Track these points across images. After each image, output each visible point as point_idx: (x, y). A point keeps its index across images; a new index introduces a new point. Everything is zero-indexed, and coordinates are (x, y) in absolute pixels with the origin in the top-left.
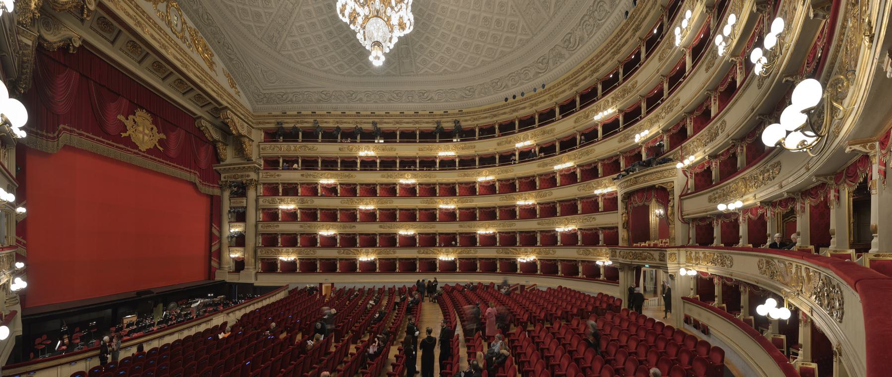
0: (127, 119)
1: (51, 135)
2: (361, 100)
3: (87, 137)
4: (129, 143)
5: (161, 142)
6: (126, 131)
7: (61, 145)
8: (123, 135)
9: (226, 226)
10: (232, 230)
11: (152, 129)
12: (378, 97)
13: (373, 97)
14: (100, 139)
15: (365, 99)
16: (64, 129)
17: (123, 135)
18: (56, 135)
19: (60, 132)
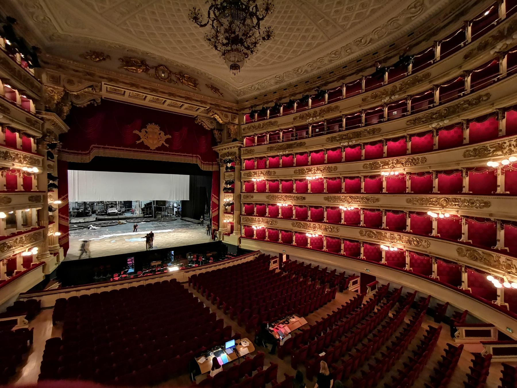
0: (140, 132)
1: (84, 152)
2: (306, 71)
3: (111, 149)
4: (143, 147)
5: (167, 141)
6: (139, 138)
7: (92, 158)
8: (138, 142)
9: (222, 194)
10: (225, 200)
11: (160, 134)
12: (319, 64)
13: (315, 65)
14: (122, 148)
15: (309, 69)
16: (94, 147)
17: (138, 142)
18: (88, 152)
19: (92, 149)
